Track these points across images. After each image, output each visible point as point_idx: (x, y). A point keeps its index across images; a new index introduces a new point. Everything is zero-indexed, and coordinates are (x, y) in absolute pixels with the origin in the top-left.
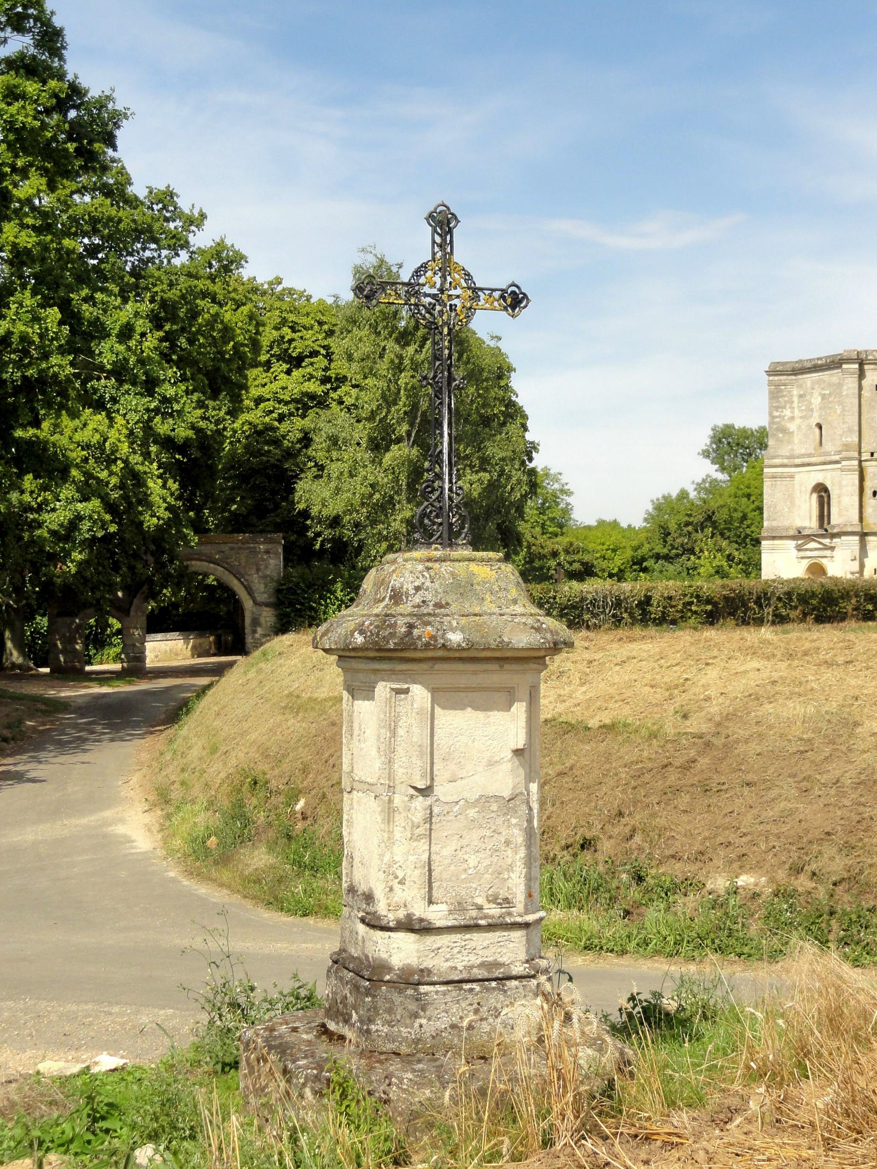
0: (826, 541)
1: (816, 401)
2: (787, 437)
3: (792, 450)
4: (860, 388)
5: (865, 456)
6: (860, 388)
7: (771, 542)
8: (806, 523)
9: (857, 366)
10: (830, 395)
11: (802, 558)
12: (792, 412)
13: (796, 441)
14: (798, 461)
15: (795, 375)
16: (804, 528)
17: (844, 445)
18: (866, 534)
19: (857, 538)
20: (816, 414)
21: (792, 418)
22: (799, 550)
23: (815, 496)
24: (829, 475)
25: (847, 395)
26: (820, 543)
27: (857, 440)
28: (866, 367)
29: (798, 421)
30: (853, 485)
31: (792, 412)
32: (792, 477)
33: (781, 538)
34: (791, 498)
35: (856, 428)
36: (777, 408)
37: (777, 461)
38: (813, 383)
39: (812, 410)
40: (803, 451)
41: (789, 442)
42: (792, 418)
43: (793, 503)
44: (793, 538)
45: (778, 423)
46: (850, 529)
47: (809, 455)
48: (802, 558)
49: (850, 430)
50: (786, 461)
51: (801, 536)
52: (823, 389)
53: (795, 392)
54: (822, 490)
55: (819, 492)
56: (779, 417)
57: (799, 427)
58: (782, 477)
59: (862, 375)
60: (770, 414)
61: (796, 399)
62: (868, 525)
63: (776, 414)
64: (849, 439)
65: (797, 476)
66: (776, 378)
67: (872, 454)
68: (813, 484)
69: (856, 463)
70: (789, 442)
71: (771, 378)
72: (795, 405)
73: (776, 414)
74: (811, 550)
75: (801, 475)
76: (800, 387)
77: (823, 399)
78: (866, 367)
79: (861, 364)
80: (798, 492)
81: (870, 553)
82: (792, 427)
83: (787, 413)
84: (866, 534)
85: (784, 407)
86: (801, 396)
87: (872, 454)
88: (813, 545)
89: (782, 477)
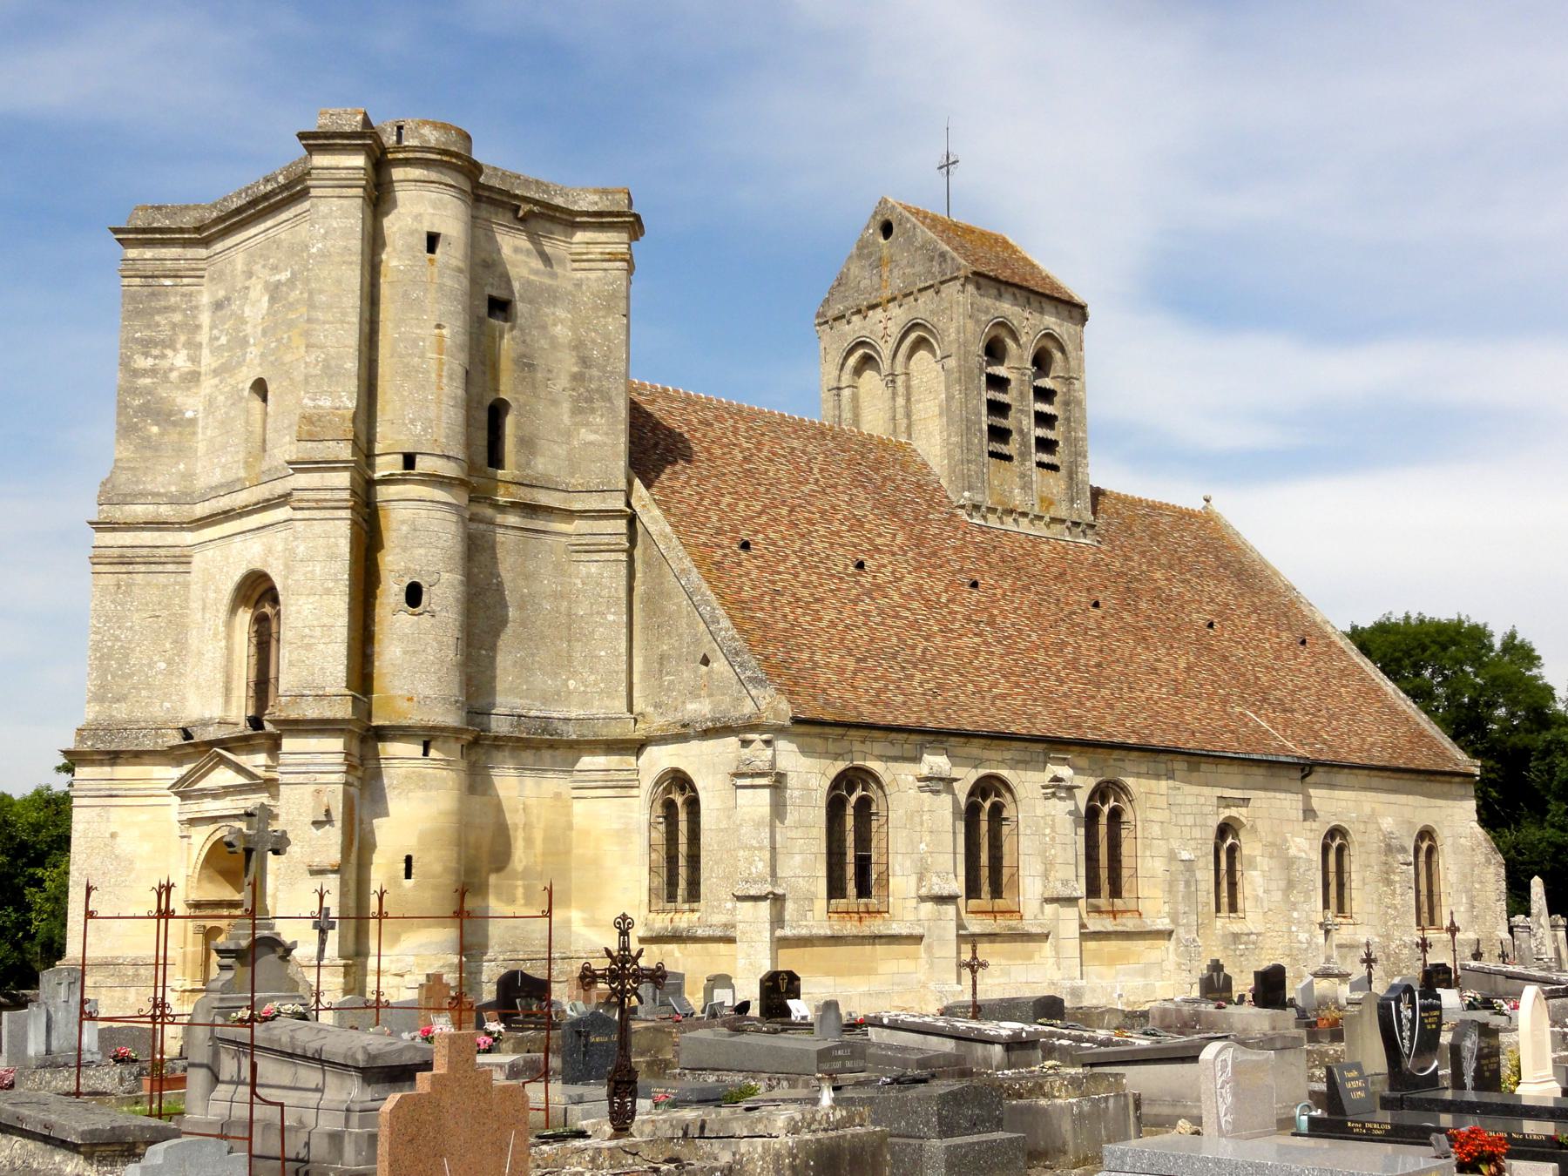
0: (257, 761)
1: (256, 308)
2: (173, 436)
3: (189, 476)
4: (374, 242)
5: (386, 465)
6: (374, 242)
7: (106, 771)
8: (215, 711)
9: (359, 160)
10: (291, 282)
11: (193, 822)
12: (194, 359)
13: (202, 448)
14: (201, 510)
15: (206, 243)
16: (205, 724)
17: (307, 419)
18: (382, 734)
19: (337, 744)
20: (253, 352)
21: (193, 378)
22: (184, 796)
23: (245, 617)
24: (278, 539)
25: (324, 255)
26: (240, 769)
27: (348, 401)
28: (398, 173)
29: (208, 384)
30: (332, 557)
31: (194, 359)
32: (183, 560)
33: (137, 756)
34: (178, 629)
35: (352, 365)
36: (146, 345)
37: (139, 511)
38: (250, 261)
39: (244, 343)
40: (217, 477)
41: (181, 451)
42: (193, 378)
43: (181, 644)
44: (170, 756)
45: (149, 391)
46: (312, 711)
47: (231, 488)
48: (193, 822)
49: (330, 370)
50: (166, 512)
51: (196, 748)
52: (275, 269)
53: (205, 299)
54: (258, 592)
55: (257, 604)
56: (153, 372)
57: (211, 402)
58: (153, 560)
59: (378, 197)
60: (125, 364)
61: (205, 318)
62: (389, 699)
63: (142, 363)
64: (325, 402)
65: (197, 559)
66: (149, 253)
67: (409, 461)
68: (237, 576)
69: (343, 479)
70: (181, 451)
71: (133, 253)
72: (203, 337)
73: (142, 363)
74: (215, 794)
75: (211, 552)
76: (218, 278)
77: (273, 300)
78: (398, 173)
79: (380, 163)
80: (195, 605)
81: (395, 803)
82: (190, 404)
83: (179, 360)
84: (382, 734)
85: (170, 344)
86: (218, 306)
87: (409, 461)
88: (222, 777)
89: (153, 560)
